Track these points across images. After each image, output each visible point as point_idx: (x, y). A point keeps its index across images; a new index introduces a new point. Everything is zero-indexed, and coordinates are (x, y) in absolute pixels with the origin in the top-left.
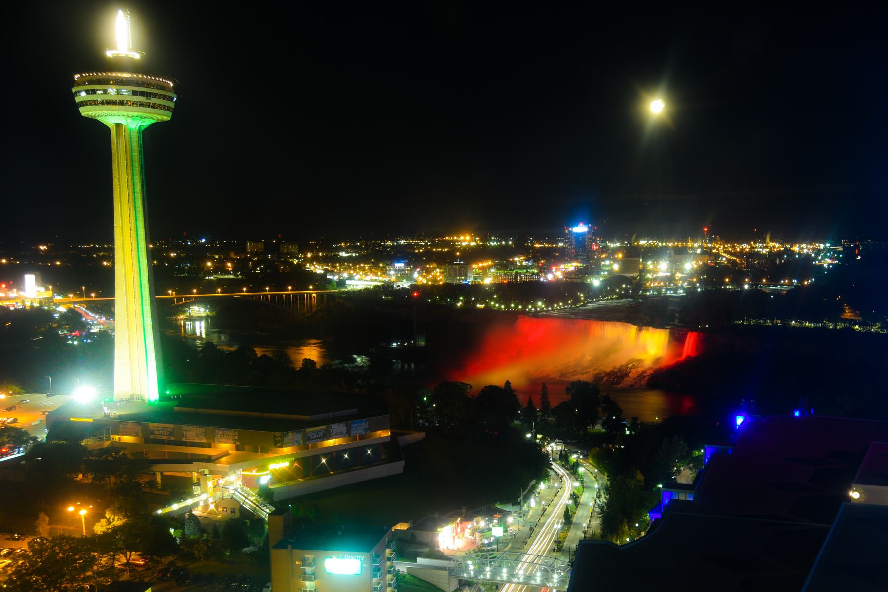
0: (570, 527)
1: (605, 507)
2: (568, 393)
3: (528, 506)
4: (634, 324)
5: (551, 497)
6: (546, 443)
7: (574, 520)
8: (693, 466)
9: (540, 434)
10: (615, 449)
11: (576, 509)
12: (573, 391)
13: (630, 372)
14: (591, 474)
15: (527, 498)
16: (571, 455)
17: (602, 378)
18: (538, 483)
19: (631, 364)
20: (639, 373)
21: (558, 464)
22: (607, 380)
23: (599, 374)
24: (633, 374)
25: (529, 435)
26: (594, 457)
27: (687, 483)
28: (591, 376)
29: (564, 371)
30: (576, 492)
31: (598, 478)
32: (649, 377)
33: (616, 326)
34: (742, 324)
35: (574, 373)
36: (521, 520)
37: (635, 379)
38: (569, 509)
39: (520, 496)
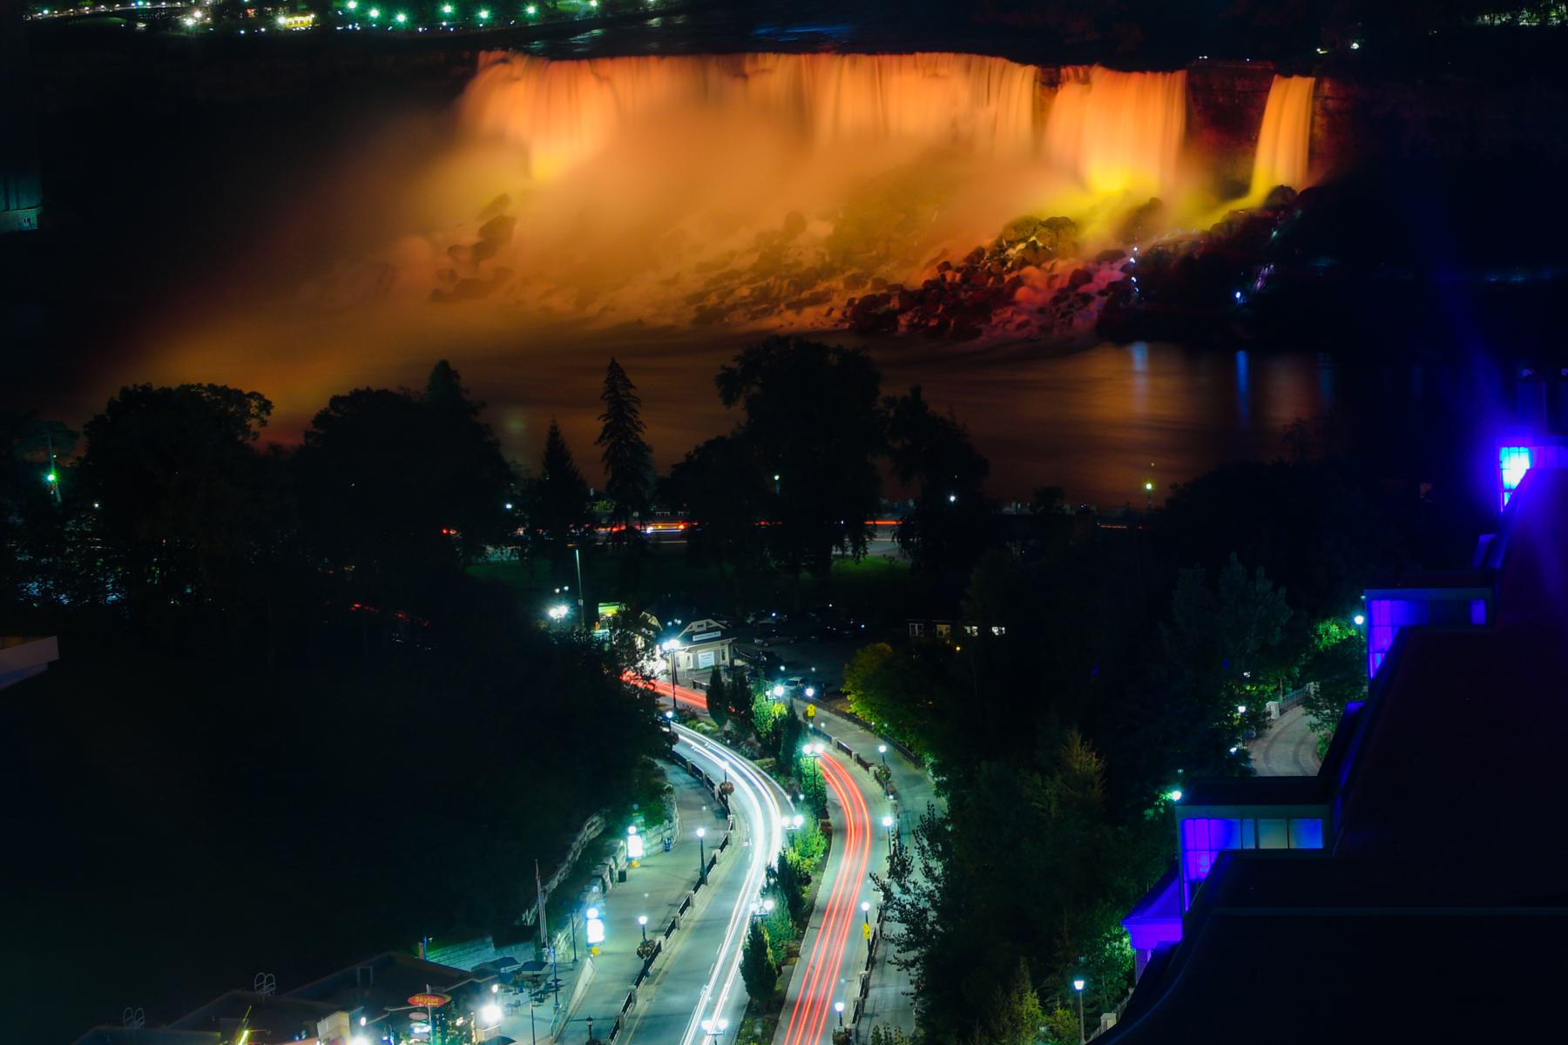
0: (775, 1023)
1: (932, 915)
2: (729, 400)
3: (574, 945)
4: (1021, 58)
5: (676, 892)
6: (640, 642)
7: (794, 989)
8: (1323, 691)
9: (609, 600)
10: (965, 639)
11: (799, 938)
12: (755, 389)
13: (1018, 282)
14: (859, 767)
15: (564, 906)
16: (761, 690)
17: (892, 317)
18: (614, 830)
19: (1022, 246)
20: (1057, 284)
21: (705, 733)
22: (911, 326)
23: (870, 302)
24: (1035, 289)
25: (559, 612)
26: (868, 688)
27: (1301, 775)
28: (836, 314)
29: (713, 299)
30: (793, 856)
31: (896, 782)
32: (1106, 298)
33: (942, 71)
34: (1511, 27)
35: (755, 303)
36: (546, 1010)
37: (1041, 310)
38: (767, 937)
39: (530, 902)
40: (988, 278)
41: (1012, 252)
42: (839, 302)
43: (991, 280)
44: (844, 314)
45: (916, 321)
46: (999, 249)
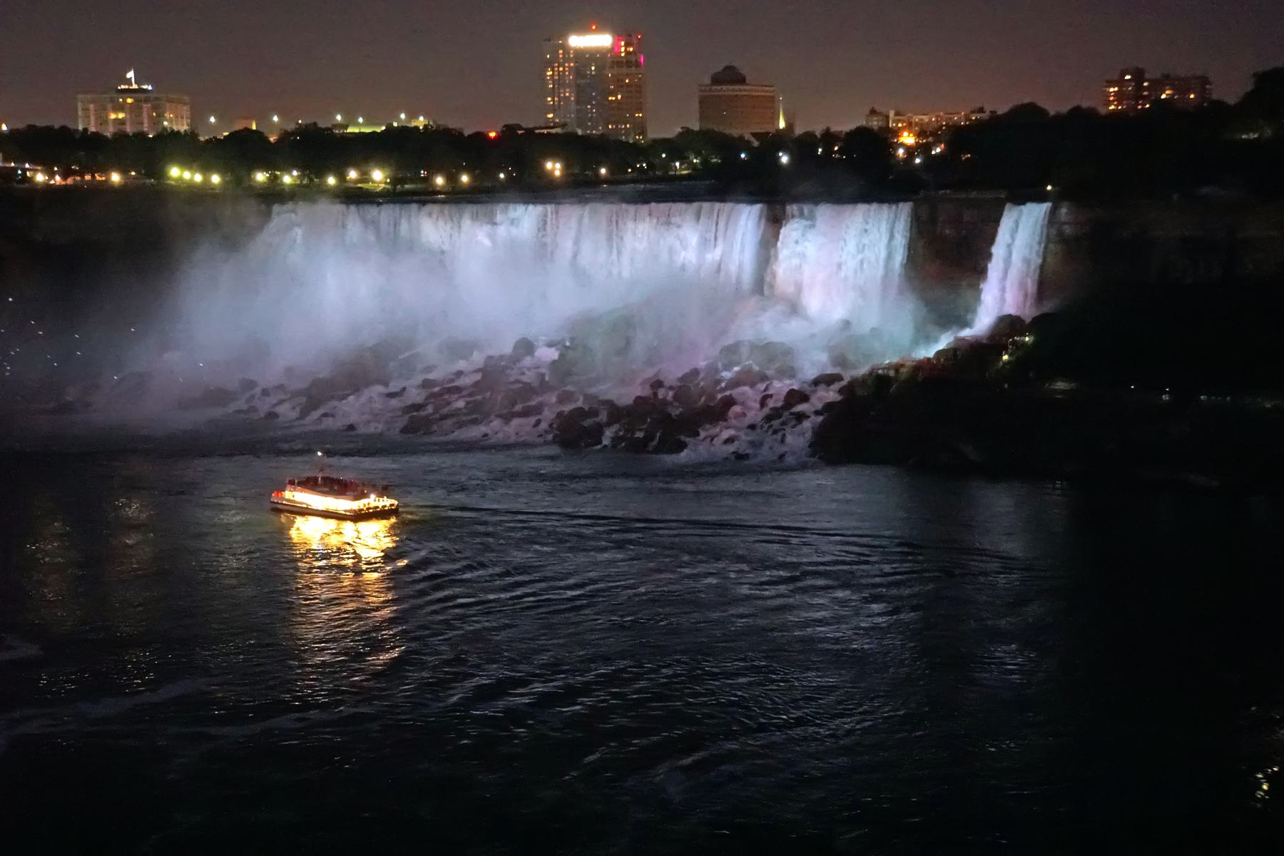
13: (729, 402)
20: (771, 403)
22: (616, 440)
23: (580, 413)
28: (544, 426)
32: (820, 419)
40: (700, 397)
41: (727, 375)
42: (548, 415)
43: (703, 399)
44: (551, 426)
45: (621, 433)
46: (713, 370)
